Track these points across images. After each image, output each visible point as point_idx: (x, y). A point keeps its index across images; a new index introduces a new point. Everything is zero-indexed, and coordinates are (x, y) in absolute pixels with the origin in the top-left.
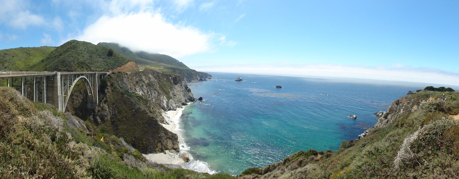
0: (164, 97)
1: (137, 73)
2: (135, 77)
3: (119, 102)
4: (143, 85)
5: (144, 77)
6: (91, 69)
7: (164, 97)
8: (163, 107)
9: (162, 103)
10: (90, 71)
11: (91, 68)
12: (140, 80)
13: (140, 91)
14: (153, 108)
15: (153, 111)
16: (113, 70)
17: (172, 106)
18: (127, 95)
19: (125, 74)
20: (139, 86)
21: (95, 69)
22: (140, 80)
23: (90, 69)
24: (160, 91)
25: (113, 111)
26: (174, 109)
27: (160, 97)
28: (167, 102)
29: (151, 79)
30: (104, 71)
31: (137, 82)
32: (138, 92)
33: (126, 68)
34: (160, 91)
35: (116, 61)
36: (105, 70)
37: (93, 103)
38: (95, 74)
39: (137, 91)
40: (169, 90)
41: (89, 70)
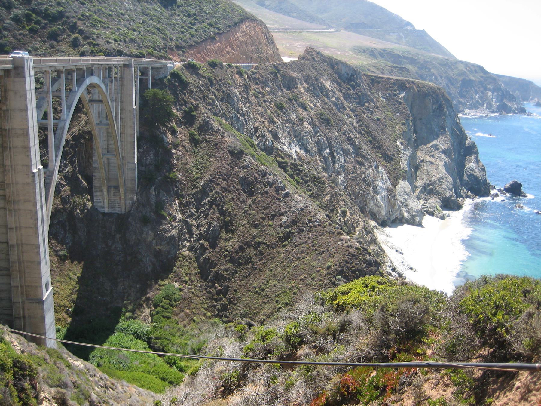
0: (380, 169)
1: (279, 70)
2: (271, 84)
3: (224, 184)
4: (301, 120)
5: (306, 86)
6: (98, 45)
7: (378, 172)
8: (376, 209)
9: (372, 192)
10: (93, 53)
11: (94, 42)
12: (290, 99)
13: (290, 143)
14: (344, 213)
15: (345, 223)
16: (184, 52)
17: (406, 206)
18: (253, 156)
19: (235, 70)
20: (288, 121)
21: (115, 46)
22: (290, 99)
23: (90, 44)
24: (365, 148)
25: (202, 221)
26: (414, 220)
27: (363, 169)
28: (388, 190)
29: (330, 93)
30: (150, 55)
31: (280, 107)
32: (285, 145)
33: (235, 47)
34: (365, 148)
35: (194, 14)
36: (155, 53)
37: (117, 188)
38: (125, 66)
39: (280, 142)
40: (398, 143)
41: (86, 48)
